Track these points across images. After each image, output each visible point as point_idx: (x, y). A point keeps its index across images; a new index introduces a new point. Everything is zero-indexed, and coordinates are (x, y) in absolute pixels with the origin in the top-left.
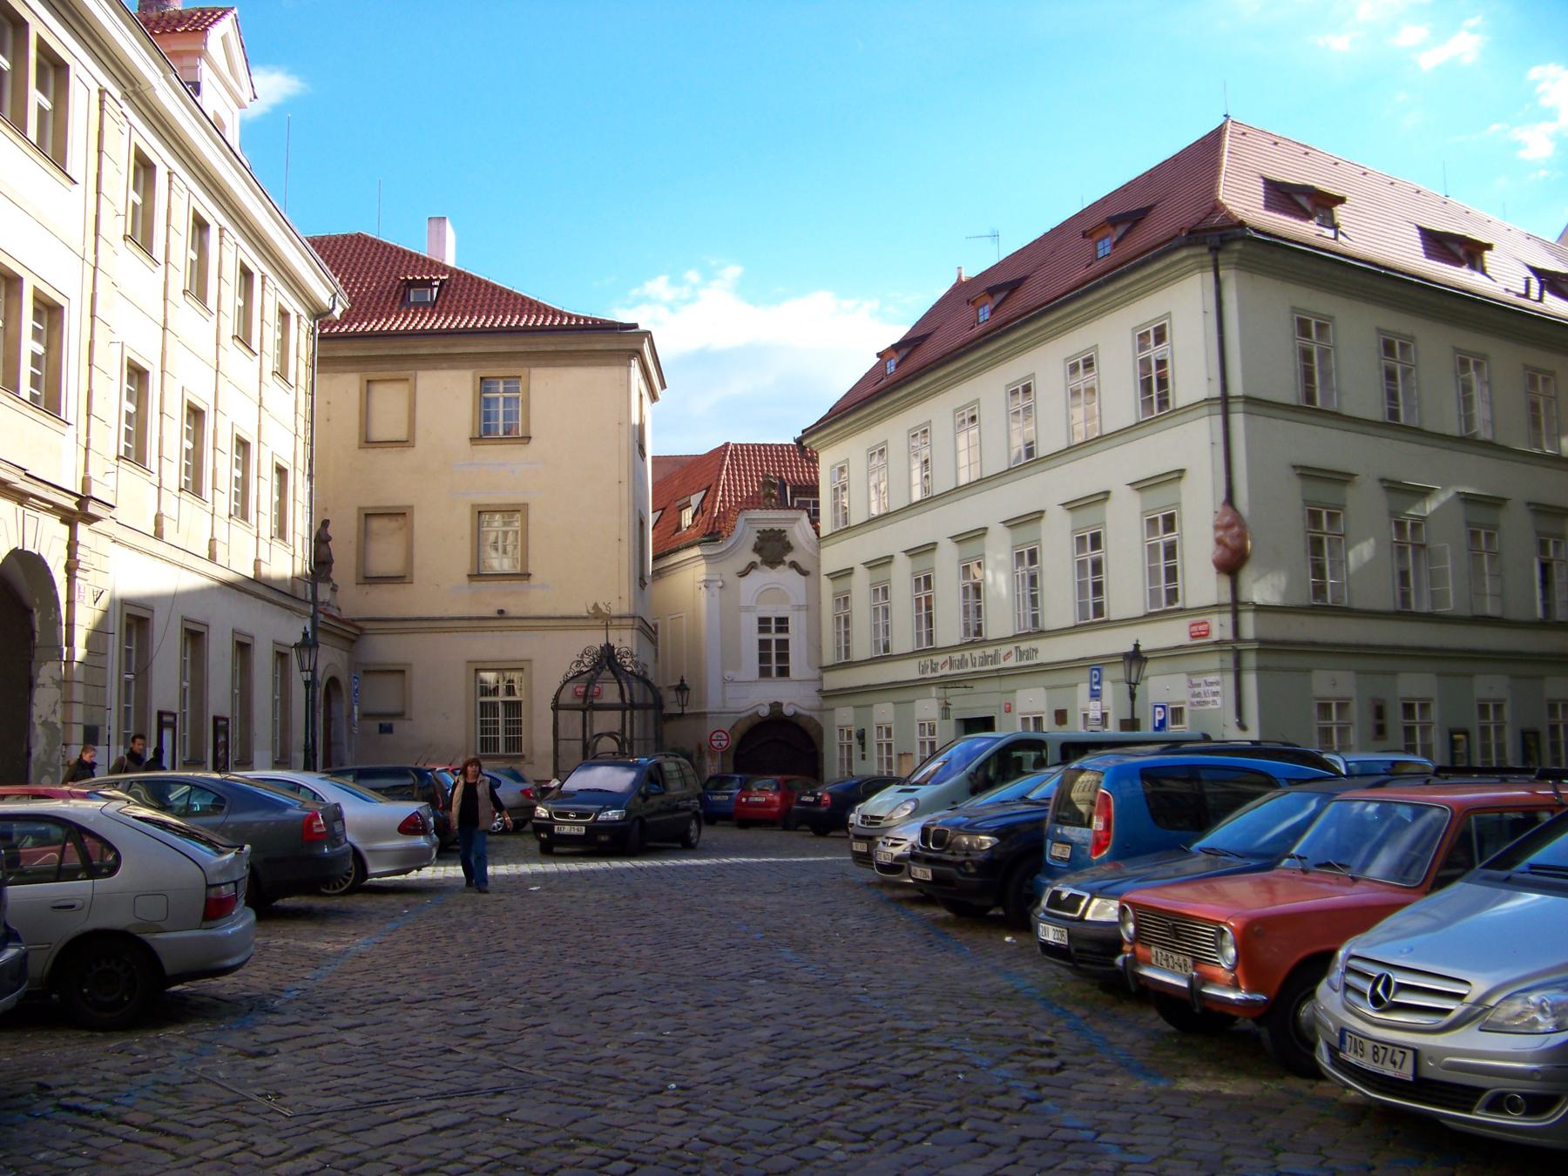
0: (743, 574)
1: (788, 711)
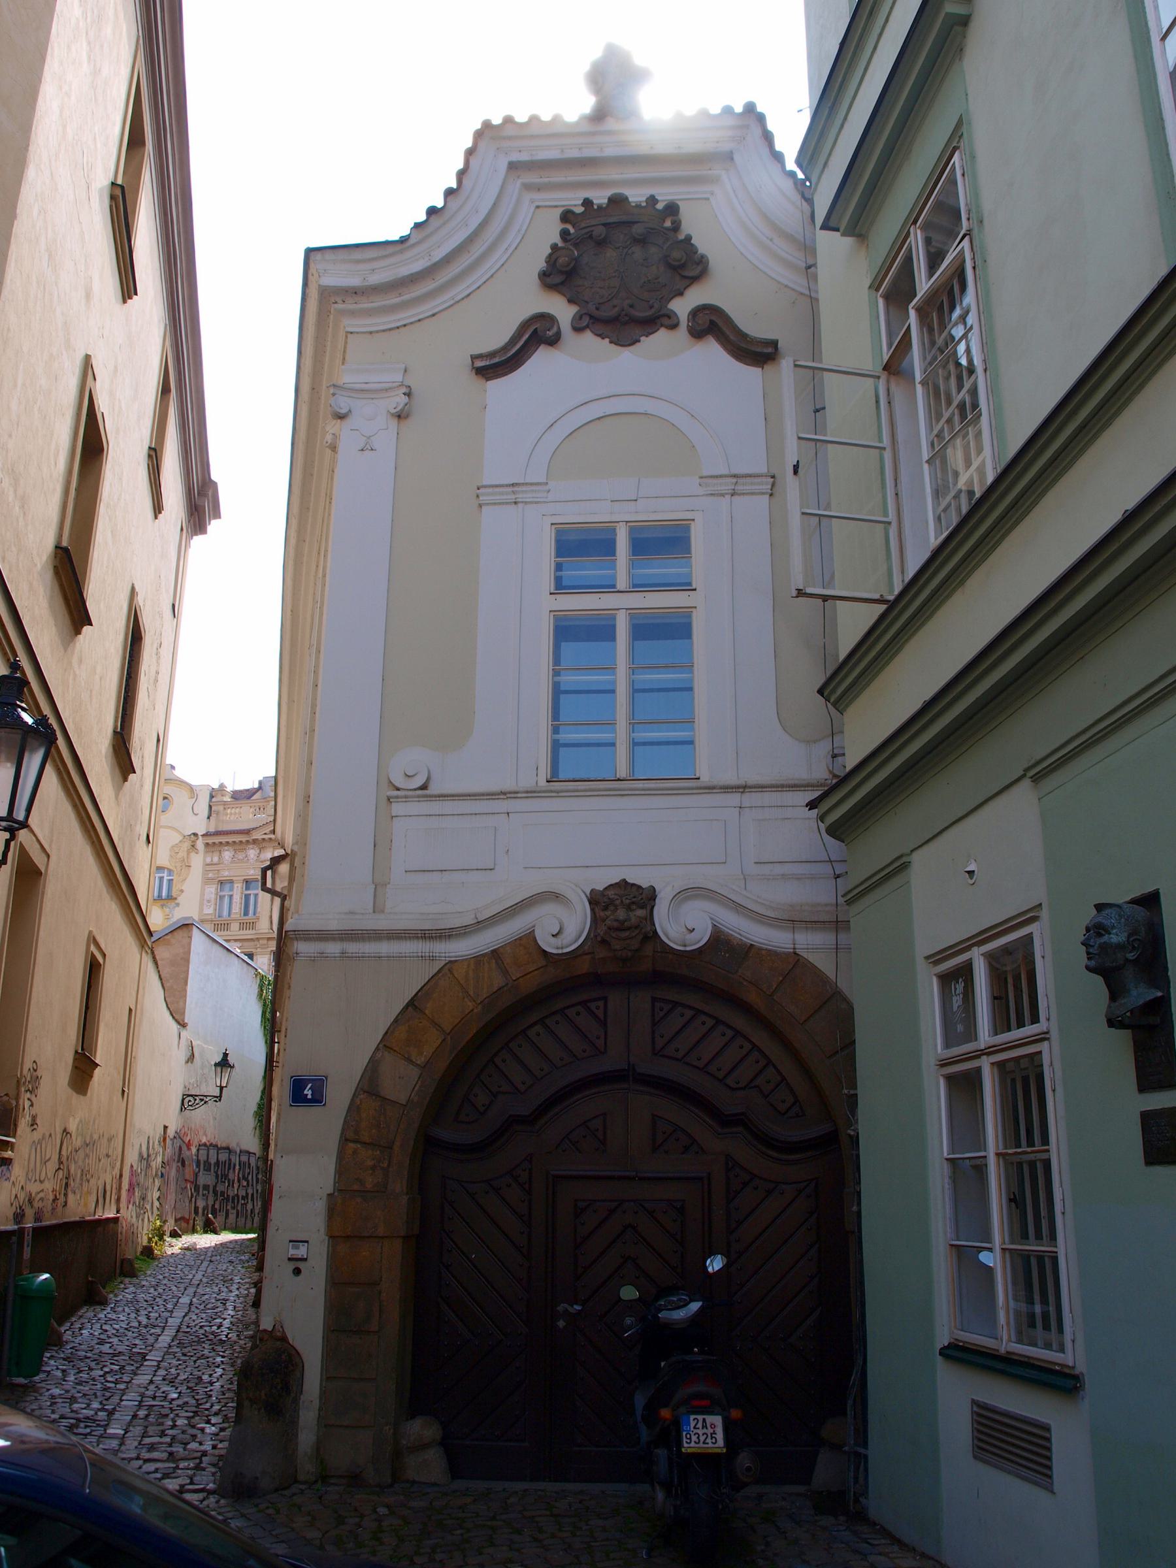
0: (496, 366)
1: (681, 926)
